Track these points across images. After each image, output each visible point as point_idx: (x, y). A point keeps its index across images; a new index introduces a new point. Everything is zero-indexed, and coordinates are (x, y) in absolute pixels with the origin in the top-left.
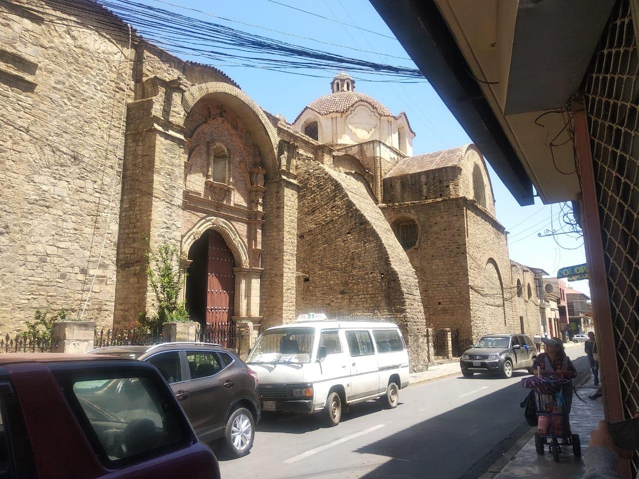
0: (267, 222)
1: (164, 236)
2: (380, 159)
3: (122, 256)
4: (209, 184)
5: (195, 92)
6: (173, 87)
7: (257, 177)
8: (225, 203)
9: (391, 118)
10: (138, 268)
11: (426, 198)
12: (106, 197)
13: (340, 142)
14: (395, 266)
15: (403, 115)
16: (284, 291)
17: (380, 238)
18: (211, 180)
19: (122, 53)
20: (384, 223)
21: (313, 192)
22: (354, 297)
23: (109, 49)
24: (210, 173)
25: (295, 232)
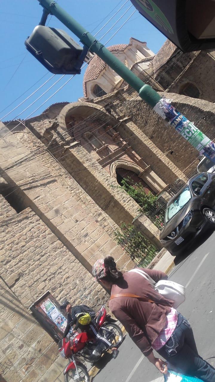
0: (133, 145)
1: (109, 184)
2: (144, 71)
3: (102, 206)
5: (61, 120)
6: (55, 126)
8: (110, 154)
10: (112, 203)
11: (184, 67)
13: (116, 83)
14: (206, 109)
15: (132, 40)
17: (188, 104)
18: (97, 150)
19: (25, 133)
20: (181, 97)
21: (138, 115)
23: (21, 136)
24: (95, 148)
25: (147, 138)
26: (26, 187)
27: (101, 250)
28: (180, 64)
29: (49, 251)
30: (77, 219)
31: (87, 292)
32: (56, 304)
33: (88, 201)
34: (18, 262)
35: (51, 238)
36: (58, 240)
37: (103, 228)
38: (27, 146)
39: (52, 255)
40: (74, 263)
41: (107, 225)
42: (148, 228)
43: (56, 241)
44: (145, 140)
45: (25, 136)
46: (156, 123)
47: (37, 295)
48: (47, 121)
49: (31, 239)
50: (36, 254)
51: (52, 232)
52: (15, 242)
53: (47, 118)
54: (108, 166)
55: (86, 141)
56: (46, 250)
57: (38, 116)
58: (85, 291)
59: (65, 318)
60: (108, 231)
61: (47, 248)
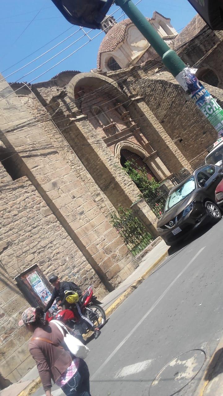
0: (142, 127)
1: (112, 165)
3: (101, 186)
4: (105, 129)
5: (70, 89)
6: (62, 95)
7: (120, 109)
8: (117, 133)
9: (151, 21)
10: (113, 185)
11: (207, 51)
12: (76, 166)
13: (133, 58)
15: (156, 14)
16: (174, 153)
19: (30, 98)
21: (152, 95)
22: (212, 131)
23: (25, 100)
24: (102, 124)
25: (158, 122)
26: (25, 154)
27: (95, 231)
28: (202, 47)
29: (41, 224)
30: (74, 195)
31: (76, 270)
32: (42, 278)
33: (88, 179)
34: (9, 230)
35: (46, 211)
36: (52, 213)
37: (100, 209)
38: (30, 113)
39: (44, 228)
40: (66, 240)
41: (104, 207)
42: (146, 215)
43: (50, 215)
44: (155, 124)
45: (30, 101)
46: (169, 107)
47: (24, 266)
48: (54, 89)
49: (25, 208)
50: (28, 224)
51: (46, 205)
52: (8, 210)
53: (55, 85)
54: (112, 145)
55: (94, 115)
56: (39, 222)
57: (46, 81)
58: (73, 268)
59: (50, 293)
60: (104, 212)
61: (40, 220)
